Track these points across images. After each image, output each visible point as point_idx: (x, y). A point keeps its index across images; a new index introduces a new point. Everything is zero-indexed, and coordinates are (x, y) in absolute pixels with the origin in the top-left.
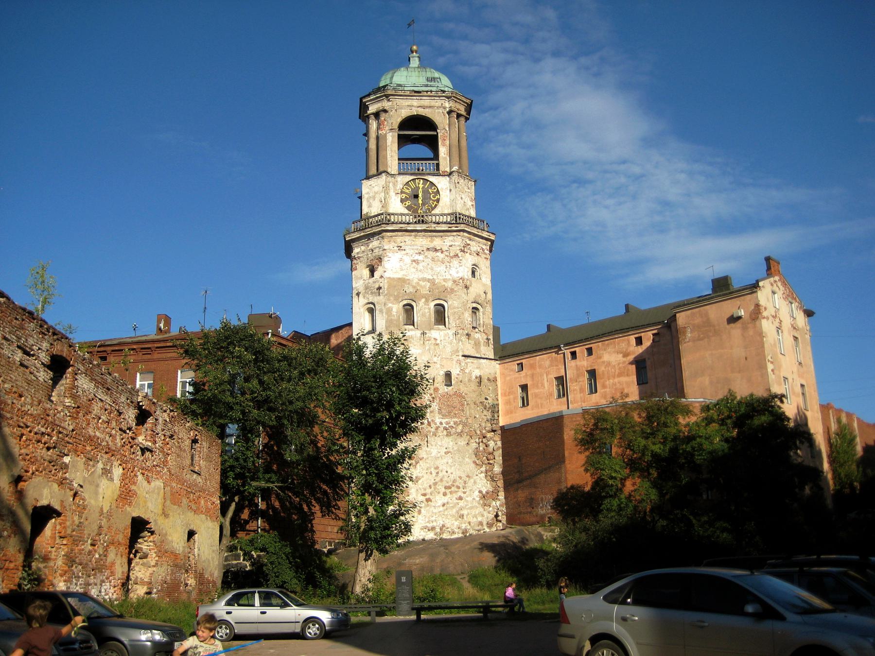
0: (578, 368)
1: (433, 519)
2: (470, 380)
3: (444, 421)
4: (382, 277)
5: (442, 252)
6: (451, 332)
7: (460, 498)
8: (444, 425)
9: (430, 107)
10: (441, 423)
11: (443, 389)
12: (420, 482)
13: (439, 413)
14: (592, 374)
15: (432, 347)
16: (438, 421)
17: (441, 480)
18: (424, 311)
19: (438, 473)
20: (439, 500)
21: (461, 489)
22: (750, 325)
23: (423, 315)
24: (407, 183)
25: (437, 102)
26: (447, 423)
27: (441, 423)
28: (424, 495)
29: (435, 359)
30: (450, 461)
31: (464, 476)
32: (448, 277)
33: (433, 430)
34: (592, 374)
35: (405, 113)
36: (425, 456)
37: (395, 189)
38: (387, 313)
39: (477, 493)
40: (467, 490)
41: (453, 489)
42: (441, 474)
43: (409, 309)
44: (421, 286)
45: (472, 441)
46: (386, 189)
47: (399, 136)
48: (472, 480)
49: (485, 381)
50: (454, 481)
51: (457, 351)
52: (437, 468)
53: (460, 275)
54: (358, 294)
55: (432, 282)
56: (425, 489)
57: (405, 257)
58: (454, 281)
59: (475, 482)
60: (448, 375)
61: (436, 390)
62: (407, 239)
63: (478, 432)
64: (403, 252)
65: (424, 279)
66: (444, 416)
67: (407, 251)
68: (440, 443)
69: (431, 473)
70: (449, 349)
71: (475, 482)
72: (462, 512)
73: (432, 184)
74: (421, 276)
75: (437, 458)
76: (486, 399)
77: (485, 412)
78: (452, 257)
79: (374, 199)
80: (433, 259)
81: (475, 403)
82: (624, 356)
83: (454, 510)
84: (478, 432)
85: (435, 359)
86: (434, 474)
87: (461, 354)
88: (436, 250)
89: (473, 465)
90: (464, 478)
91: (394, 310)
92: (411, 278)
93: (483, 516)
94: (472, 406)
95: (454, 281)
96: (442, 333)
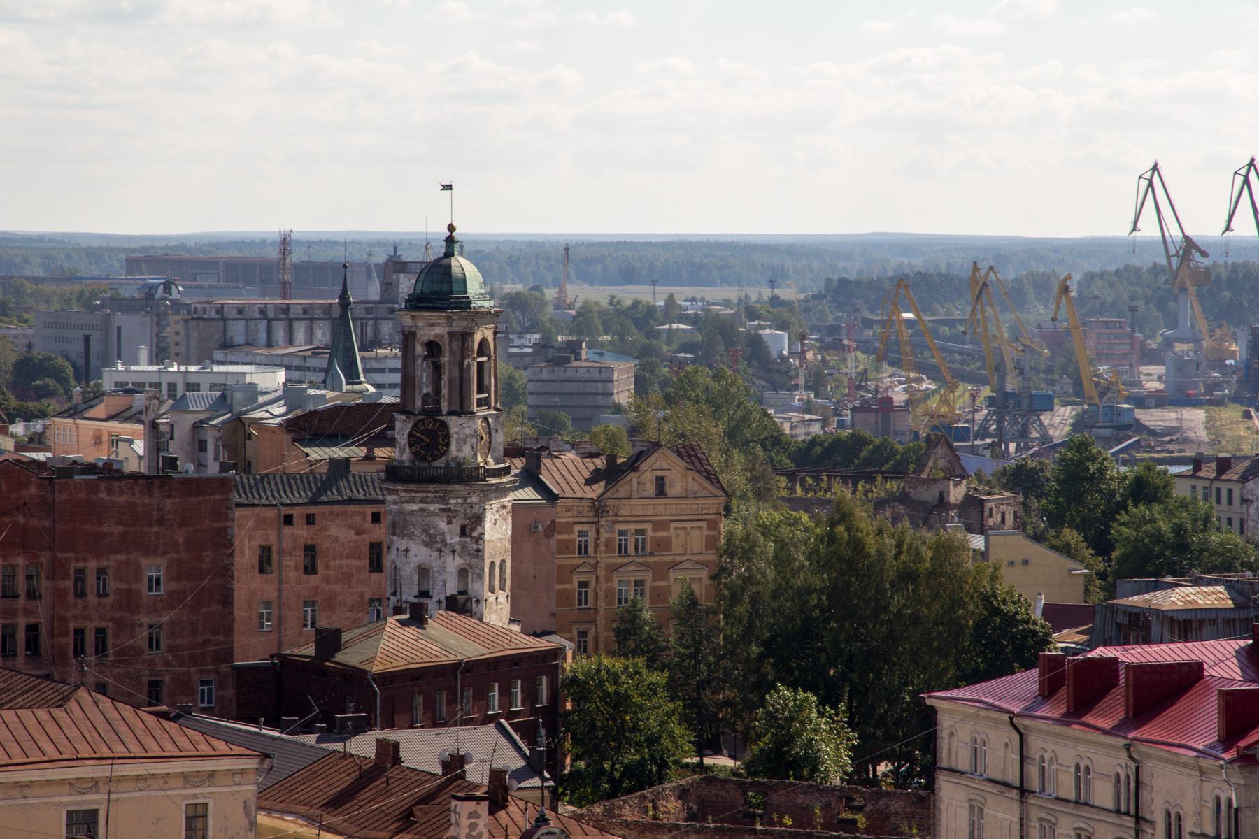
0: (294, 538)
14: (310, 550)
34: (310, 550)
54: (454, 552)
82: (357, 534)
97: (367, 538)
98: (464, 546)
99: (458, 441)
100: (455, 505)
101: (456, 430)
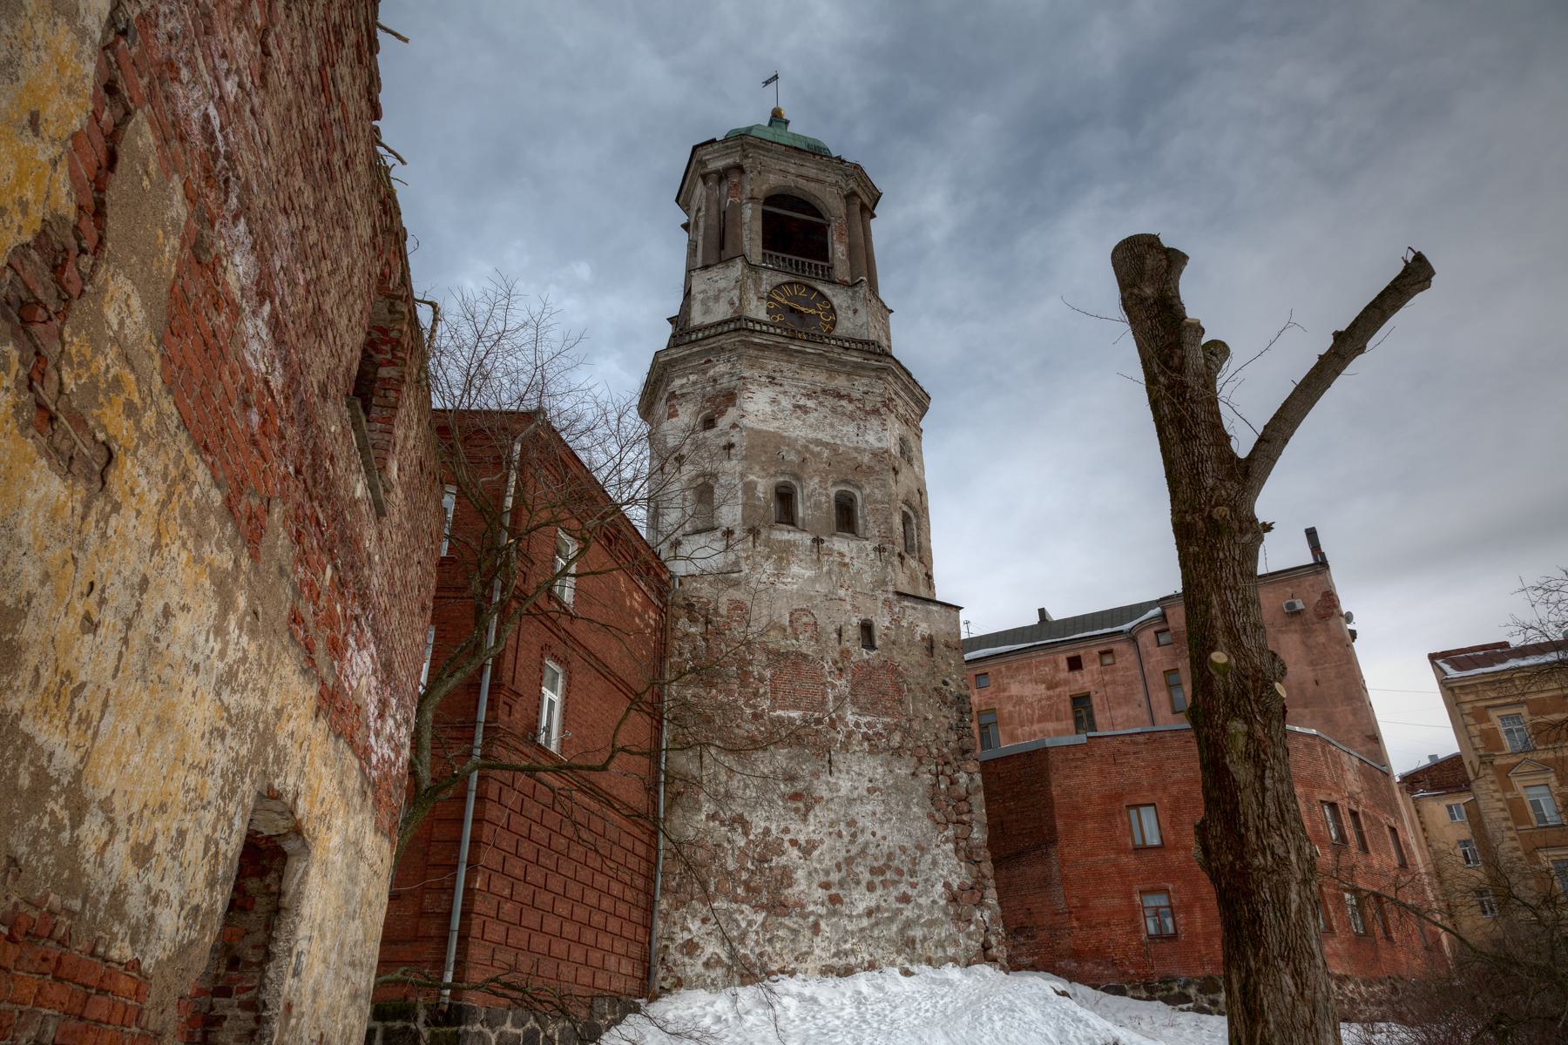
1: (848, 946)
2: (911, 643)
3: (863, 720)
4: (734, 426)
5: (851, 401)
6: (869, 546)
7: (905, 899)
8: (864, 729)
9: (818, 181)
10: (857, 725)
11: (861, 654)
12: (816, 853)
13: (854, 703)
15: (836, 569)
16: (850, 718)
17: (863, 852)
18: (815, 497)
19: (854, 835)
20: (862, 901)
21: (906, 877)
22: (1317, 626)
23: (817, 505)
24: (778, 287)
26: (869, 725)
27: (857, 725)
28: (826, 886)
29: (842, 593)
30: (880, 809)
31: (909, 844)
32: (863, 446)
33: (840, 737)
35: (773, 180)
36: (826, 794)
37: (757, 291)
38: (745, 492)
39: (939, 888)
40: (920, 879)
41: (889, 875)
42: (861, 839)
43: (785, 497)
44: (812, 453)
45: (923, 769)
46: (741, 285)
48: (928, 858)
49: (940, 648)
50: (890, 856)
51: (884, 583)
52: (852, 823)
53: (884, 445)
55: (834, 448)
56: (827, 873)
57: (781, 397)
58: (875, 455)
59: (935, 863)
60: (867, 628)
61: (845, 654)
63: (935, 751)
64: (778, 389)
65: (818, 442)
66: (863, 710)
67: (787, 388)
68: (856, 768)
69: (840, 835)
70: (867, 578)
71: (935, 863)
72: (911, 933)
73: (822, 296)
74: (812, 435)
75: (851, 801)
76: (945, 683)
77: (945, 711)
78: (867, 413)
79: (717, 299)
80: (834, 410)
81: (923, 690)
82: (1048, 688)
83: (894, 928)
84: (935, 751)
85: (842, 593)
86: (847, 839)
87: (891, 588)
88: (840, 396)
89: (928, 822)
90: (912, 851)
91: (760, 488)
92: (793, 435)
93: (956, 943)
94: (920, 695)
95: (875, 455)
96: (853, 544)
97: (1066, 692)
99: (704, 302)
100: (682, 386)
101: (703, 287)
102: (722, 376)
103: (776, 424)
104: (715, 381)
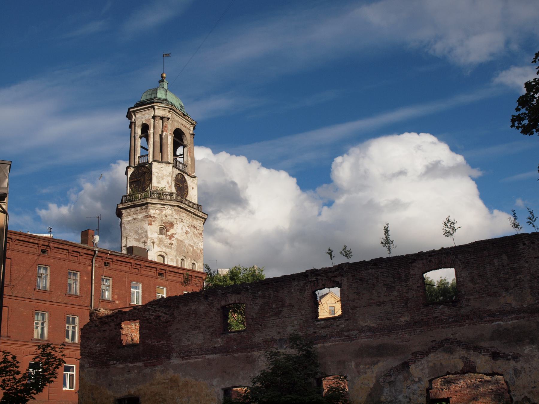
25: (188, 125)
47: (174, 140)
54: (153, 243)
57: (183, 227)
62: (184, 215)
64: (183, 224)
65: (190, 245)
73: (185, 181)
88: (195, 228)
98: (160, 240)
99: (158, 177)
100: (154, 214)
101: (157, 171)
102: (169, 215)
103: (183, 237)
104: (166, 216)
